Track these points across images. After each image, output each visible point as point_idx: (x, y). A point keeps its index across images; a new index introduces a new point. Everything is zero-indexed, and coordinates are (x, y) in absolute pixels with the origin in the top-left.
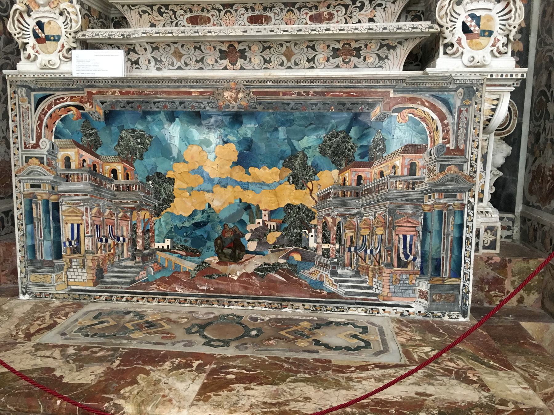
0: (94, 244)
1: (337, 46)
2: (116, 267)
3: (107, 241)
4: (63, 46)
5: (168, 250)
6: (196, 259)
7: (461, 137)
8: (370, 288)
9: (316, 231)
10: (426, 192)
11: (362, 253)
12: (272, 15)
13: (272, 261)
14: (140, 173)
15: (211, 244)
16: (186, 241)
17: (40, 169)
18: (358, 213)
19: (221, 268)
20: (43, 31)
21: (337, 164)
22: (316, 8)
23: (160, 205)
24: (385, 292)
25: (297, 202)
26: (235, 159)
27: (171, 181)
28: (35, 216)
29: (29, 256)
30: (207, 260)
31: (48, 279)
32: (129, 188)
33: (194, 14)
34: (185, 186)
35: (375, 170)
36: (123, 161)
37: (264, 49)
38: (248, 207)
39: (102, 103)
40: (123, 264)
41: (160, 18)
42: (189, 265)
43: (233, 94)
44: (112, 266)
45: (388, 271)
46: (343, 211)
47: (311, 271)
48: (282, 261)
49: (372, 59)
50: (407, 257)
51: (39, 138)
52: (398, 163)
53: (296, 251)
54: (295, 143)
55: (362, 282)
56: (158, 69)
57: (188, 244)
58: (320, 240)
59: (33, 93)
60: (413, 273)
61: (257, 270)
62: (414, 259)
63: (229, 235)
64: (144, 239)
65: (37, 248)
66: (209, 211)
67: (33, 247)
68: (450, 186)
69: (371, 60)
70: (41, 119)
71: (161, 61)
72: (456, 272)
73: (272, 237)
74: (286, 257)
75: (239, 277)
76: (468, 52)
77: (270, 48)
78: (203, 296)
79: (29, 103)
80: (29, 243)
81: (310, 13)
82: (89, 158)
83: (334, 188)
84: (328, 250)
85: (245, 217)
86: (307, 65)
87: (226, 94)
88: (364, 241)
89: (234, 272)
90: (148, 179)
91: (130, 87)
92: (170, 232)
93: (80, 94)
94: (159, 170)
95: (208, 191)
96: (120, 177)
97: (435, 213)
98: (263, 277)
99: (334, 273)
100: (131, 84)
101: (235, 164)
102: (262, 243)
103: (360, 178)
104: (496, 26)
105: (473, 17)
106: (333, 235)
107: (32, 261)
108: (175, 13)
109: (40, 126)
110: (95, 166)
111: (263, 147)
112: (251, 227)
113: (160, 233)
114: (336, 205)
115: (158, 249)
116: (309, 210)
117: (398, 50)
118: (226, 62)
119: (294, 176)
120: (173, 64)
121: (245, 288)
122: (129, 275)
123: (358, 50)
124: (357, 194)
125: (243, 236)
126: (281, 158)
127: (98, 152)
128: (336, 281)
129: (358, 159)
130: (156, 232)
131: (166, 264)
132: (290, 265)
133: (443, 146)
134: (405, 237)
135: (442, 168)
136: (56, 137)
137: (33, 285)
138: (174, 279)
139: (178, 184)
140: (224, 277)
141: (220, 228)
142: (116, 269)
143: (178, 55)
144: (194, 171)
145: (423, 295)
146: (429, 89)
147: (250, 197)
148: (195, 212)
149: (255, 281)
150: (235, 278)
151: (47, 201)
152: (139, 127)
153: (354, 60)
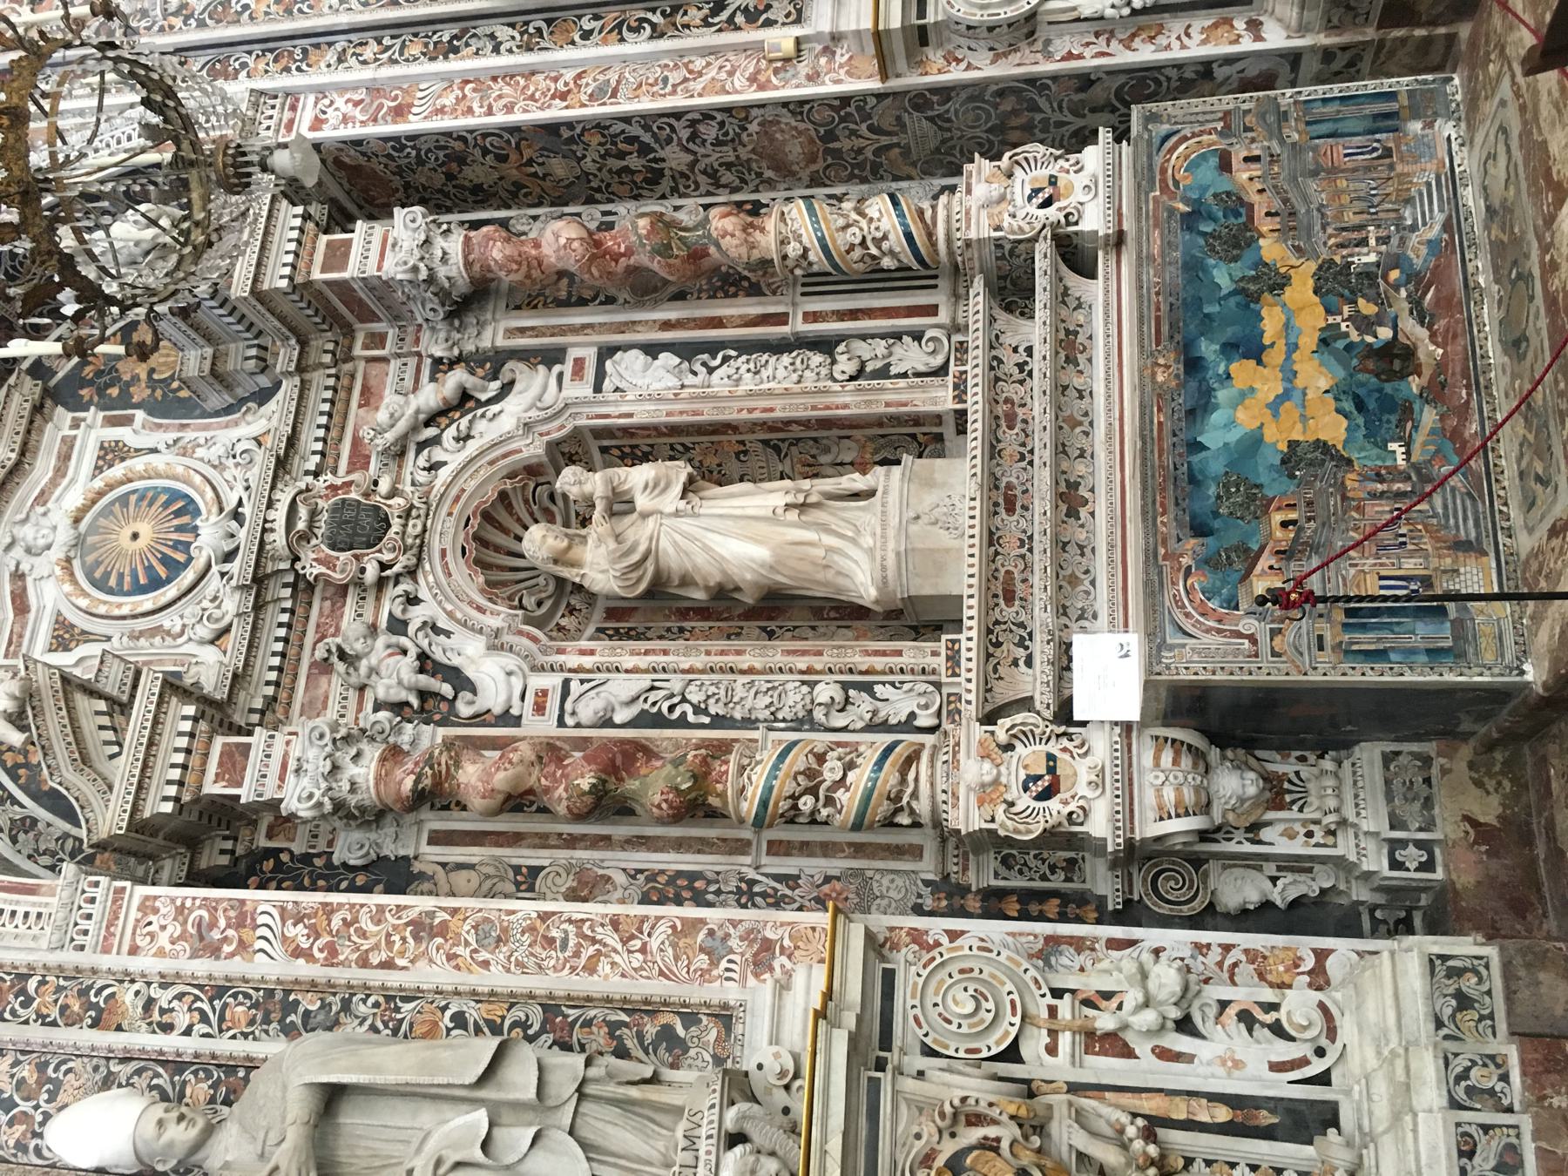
0: (1411, 554)
1: (1062, 355)
2: (1447, 520)
3: (1403, 535)
4: (1065, 750)
5: (1408, 445)
6: (1416, 407)
7: (1208, 117)
8: (1429, 184)
9: (1351, 255)
10: (1282, 142)
11: (1376, 200)
12: (1005, 480)
13: (1406, 306)
14: (1284, 488)
15: (1388, 388)
16: (1388, 422)
17: (1290, 635)
18: (1318, 210)
19: (1427, 372)
20: (1040, 777)
21: (1251, 242)
22: (997, 418)
23: (1332, 459)
24: (1431, 166)
25: (1311, 283)
26: (1252, 363)
27: (1293, 445)
28: (1372, 647)
29: (1449, 660)
30: (1415, 390)
31: (1488, 630)
32: (1310, 504)
33: (1000, 593)
34: (1299, 426)
35: (1255, 198)
36: (1266, 511)
37: (1064, 452)
38: (1324, 342)
39: (1179, 540)
40: (1440, 511)
41: (1004, 647)
42: (1429, 417)
43: (1159, 371)
44: (1447, 527)
45: (1399, 168)
46: (1318, 227)
47: (1412, 255)
48: (1403, 293)
49: (1080, 317)
50: (1375, 149)
51: (1239, 635)
52: (1245, 176)
53: (1385, 277)
54: (1224, 292)
55: (1421, 195)
56: (1095, 616)
57: (1394, 418)
58: (1365, 250)
59: (1169, 641)
60: (1398, 142)
61: (1422, 324)
62: (1378, 141)
63: (1371, 365)
64: (1393, 481)
65: (1431, 646)
66: (1337, 392)
67: (1429, 652)
68: (1271, 119)
69: (1081, 319)
70: (1208, 630)
71: (1083, 610)
72: (1391, 96)
73: (1367, 308)
74: (1396, 288)
75: (1438, 346)
76: (1079, 196)
77: (1064, 445)
78: (1479, 394)
79: (1184, 646)
80: (1423, 658)
81: (1004, 427)
82: (1265, 561)
83: (1285, 241)
84: (1378, 239)
85: (1340, 344)
86: (1087, 400)
87: (1160, 378)
88: (1359, 199)
89: (1431, 354)
90: (1292, 476)
91: (1154, 502)
92: (1376, 444)
93: (1167, 570)
94: (1277, 462)
95: (1305, 394)
96: (1293, 516)
97: (1309, 128)
98: (1432, 316)
99: (1414, 228)
100: (1150, 500)
101: (1260, 362)
102: (1380, 320)
103: (1268, 214)
104: (1043, 173)
105: (1030, 198)
106: (1355, 235)
107: (1455, 654)
108: (997, 623)
109: (1219, 631)
110: (1278, 552)
111: (1230, 332)
112: (1355, 336)
113: (1378, 458)
114: (1309, 237)
115: (1408, 460)
116: (1320, 268)
117: (1069, 284)
118: (1083, 512)
119: (1271, 289)
120: (1087, 593)
121: (1455, 337)
122: (1459, 502)
123: (1068, 332)
124: (1292, 214)
125: (1370, 345)
126: (1247, 306)
127: (1255, 547)
128: (1425, 224)
129: (1243, 219)
130: (1379, 463)
131: (1432, 448)
132: (1408, 282)
133: (1221, 134)
134: (1346, 155)
135: (1247, 129)
136: (1237, 608)
137: (1502, 656)
138: (1456, 435)
139: (1297, 436)
140: (1441, 366)
141: (1362, 377)
142: (1452, 521)
143: (1074, 581)
144: (1276, 415)
145: (1430, 125)
146: (1150, 157)
147: (1309, 341)
148: (1338, 411)
149: (1440, 325)
150: (1440, 351)
151: (1345, 625)
152: (1212, 491)
153: (1081, 339)
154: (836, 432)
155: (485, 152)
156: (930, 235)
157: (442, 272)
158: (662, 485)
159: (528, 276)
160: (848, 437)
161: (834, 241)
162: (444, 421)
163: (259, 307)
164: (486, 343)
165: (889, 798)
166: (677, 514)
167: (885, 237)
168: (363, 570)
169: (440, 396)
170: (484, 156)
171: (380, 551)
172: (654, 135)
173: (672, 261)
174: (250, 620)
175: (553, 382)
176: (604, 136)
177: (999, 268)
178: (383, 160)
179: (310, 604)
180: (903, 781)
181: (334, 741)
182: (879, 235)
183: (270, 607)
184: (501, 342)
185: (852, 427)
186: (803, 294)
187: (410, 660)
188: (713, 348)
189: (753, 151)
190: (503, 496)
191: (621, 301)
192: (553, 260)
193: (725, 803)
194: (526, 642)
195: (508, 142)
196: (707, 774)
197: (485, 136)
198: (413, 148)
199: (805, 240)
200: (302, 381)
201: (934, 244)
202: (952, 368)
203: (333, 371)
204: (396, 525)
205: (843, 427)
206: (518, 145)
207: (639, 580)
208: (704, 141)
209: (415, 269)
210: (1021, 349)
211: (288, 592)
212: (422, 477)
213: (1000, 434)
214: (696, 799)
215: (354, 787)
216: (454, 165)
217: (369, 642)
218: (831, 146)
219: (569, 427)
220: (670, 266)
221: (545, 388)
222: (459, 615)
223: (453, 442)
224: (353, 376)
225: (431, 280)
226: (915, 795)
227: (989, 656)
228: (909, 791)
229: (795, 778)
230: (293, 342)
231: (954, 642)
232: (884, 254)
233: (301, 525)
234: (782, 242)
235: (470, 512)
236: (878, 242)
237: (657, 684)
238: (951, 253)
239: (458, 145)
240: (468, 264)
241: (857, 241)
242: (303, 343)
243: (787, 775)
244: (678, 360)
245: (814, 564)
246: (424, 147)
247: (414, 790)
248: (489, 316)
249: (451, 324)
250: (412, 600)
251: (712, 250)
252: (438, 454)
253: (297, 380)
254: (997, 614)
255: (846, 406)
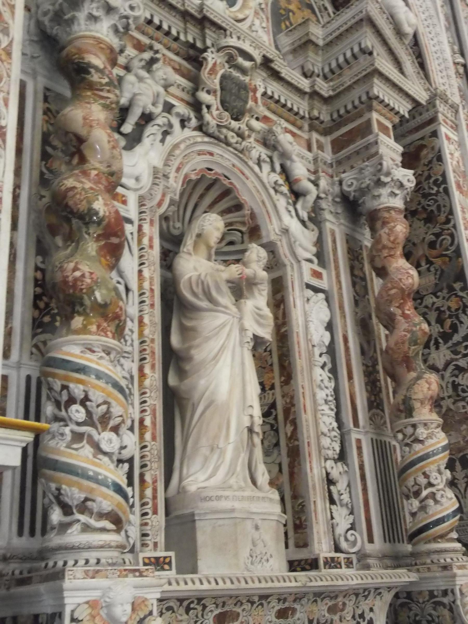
22: (336, 597)
33: (226, 608)
41: (185, 617)
81: (330, 604)
154: (285, 461)
155: (437, 235)
156: (442, 537)
157: (384, 192)
158: (262, 321)
159: (384, 247)
160: (280, 471)
161: (432, 463)
162: (284, 177)
163: (364, 73)
164: (328, 216)
165: (86, 499)
166: (243, 330)
167: (436, 502)
168: (208, 92)
169: (302, 178)
170: (433, 234)
171: (217, 109)
172: (459, 343)
173: (407, 345)
174: (179, 6)
175: (309, 256)
176: (457, 310)
177: (420, 593)
178: (426, 174)
179: (177, 54)
180: (101, 516)
181: (127, 17)
182: (438, 497)
183: (182, 25)
184: (328, 226)
185: (292, 475)
186: (372, 439)
187: (150, 108)
188: (334, 371)
189: (449, 410)
190: (238, 207)
191: (357, 310)
192: (395, 265)
193: (77, 332)
194: (158, 197)
195: (447, 249)
196: (105, 317)
197: (452, 236)
198: (438, 192)
199: (430, 441)
200: (305, 93)
201: (435, 539)
202: (342, 556)
203: (307, 116)
204: (234, 124)
205: (292, 466)
206: (446, 255)
207: (195, 294)
208: (457, 376)
209: (388, 174)
210: (371, 615)
211: (191, 40)
212: (255, 154)
213: (327, 601)
214: (82, 304)
215: (93, 18)
216: (424, 216)
217: (162, 82)
218: (458, 464)
219: (286, 262)
220: (403, 343)
221: (306, 250)
222: (177, 152)
223: (275, 179)
224: (300, 128)
225: (379, 183)
226: (87, 528)
227: (181, 601)
228: (93, 522)
229: (105, 402)
230: (331, 93)
231: (170, 563)
232: (421, 502)
233: (240, 60)
234: (425, 425)
235: (233, 181)
236: (433, 496)
237: (130, 294)
238: (429, 553)
239: (442, 218)
240: (389, 209)
241: (432, 481)
242: (326, 100)
243: (109, 394)
244: (327, 343)
245: (216, 437)
246: (439, 198)
247: (89, 65)
248: (342, 221)
249: (337, 196)
250: (183, 123)
251: (413, 375)
252: (266, 168)
253: (308, 90)
254: (211, 607)
255: (311, 469)
